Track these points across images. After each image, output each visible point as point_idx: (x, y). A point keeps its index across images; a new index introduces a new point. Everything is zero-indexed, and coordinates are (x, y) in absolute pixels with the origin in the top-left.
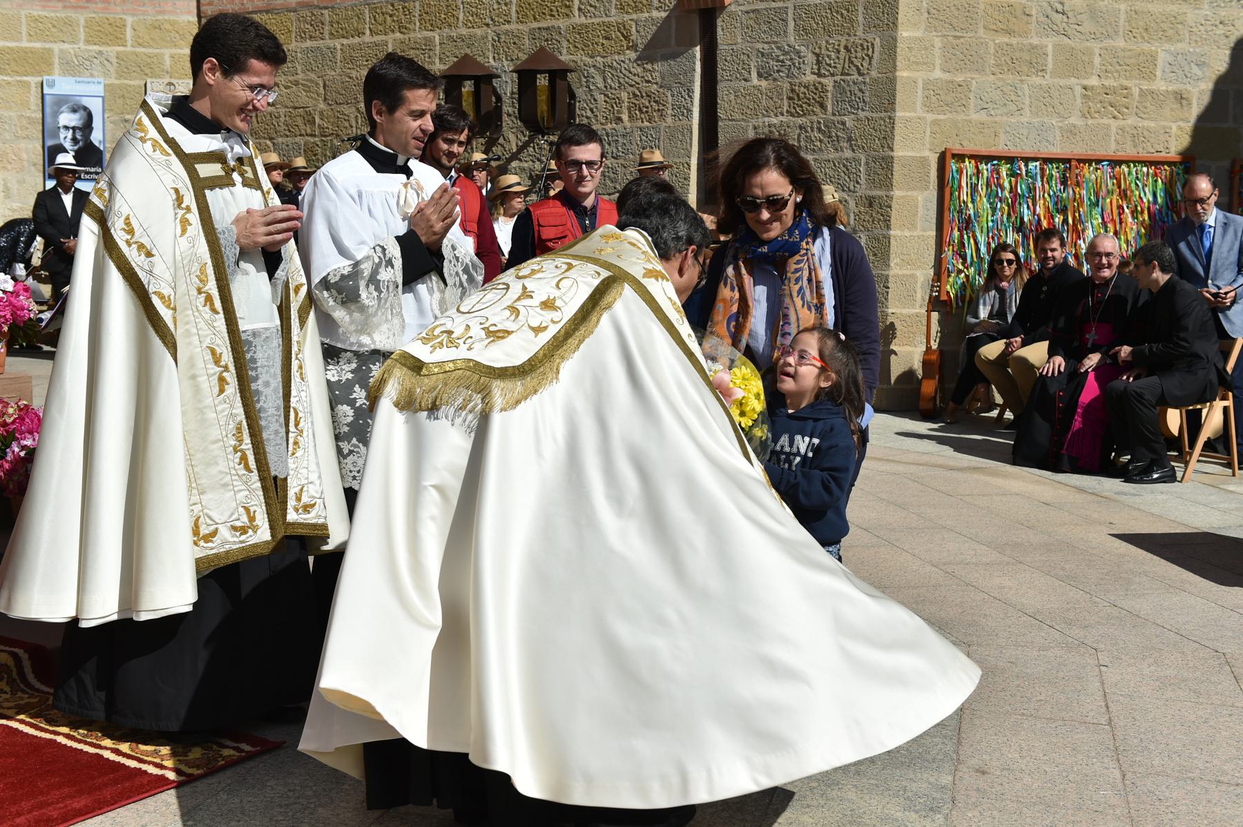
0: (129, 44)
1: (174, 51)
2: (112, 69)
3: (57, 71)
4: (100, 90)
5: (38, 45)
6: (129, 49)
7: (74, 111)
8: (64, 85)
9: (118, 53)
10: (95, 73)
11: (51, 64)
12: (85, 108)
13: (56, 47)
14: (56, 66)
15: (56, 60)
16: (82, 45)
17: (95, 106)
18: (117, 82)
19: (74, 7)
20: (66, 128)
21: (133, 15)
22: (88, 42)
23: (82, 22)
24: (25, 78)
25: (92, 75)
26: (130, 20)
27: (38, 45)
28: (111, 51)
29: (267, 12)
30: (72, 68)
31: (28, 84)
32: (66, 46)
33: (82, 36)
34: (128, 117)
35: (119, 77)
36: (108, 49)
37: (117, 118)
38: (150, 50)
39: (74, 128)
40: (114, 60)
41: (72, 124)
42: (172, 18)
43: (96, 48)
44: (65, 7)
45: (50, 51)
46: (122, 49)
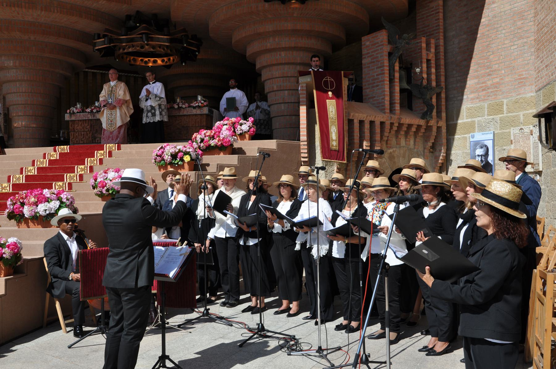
0: (505, 113)
1: (525, 112)
2: (498, 126)
3: (476, 130)
4: (491, 136)
5: (470, 120)
6: (505, 115)
7: (482, 148)
8: (478, 136)
9: (500, 118)
10: (491, 129)
11: (474, 128)
12: (486, 146)
13: (476, 120)
14: (476, 128)
15: (476, 125)
16: (486, 117)
17: (490, 144)
18: (500, 132)
19: (483, 100)
20: (479, 156)
21: (507, 98)
22: (488, 115)
23: (486, 106)
24: (465, 135)
25: (490, 130)
26: (505, 101)
27: (470, 120)
28: (497, 117)
29: (549, 84)
30: (482, 129)
31: (465, 138)
32: (480, 118)
33: (486, 113)
34: (504, 147)
35: (501, 129)
36: (496, 116)
37: (500, 149)
38: (514, 114)
39: (481, 156)
40: (499, 121)
41: (481, 154)
42: (524, 96)
43: (492, 117)
44: (480, 101)
45: (474, 121)
46: (502, 115)
